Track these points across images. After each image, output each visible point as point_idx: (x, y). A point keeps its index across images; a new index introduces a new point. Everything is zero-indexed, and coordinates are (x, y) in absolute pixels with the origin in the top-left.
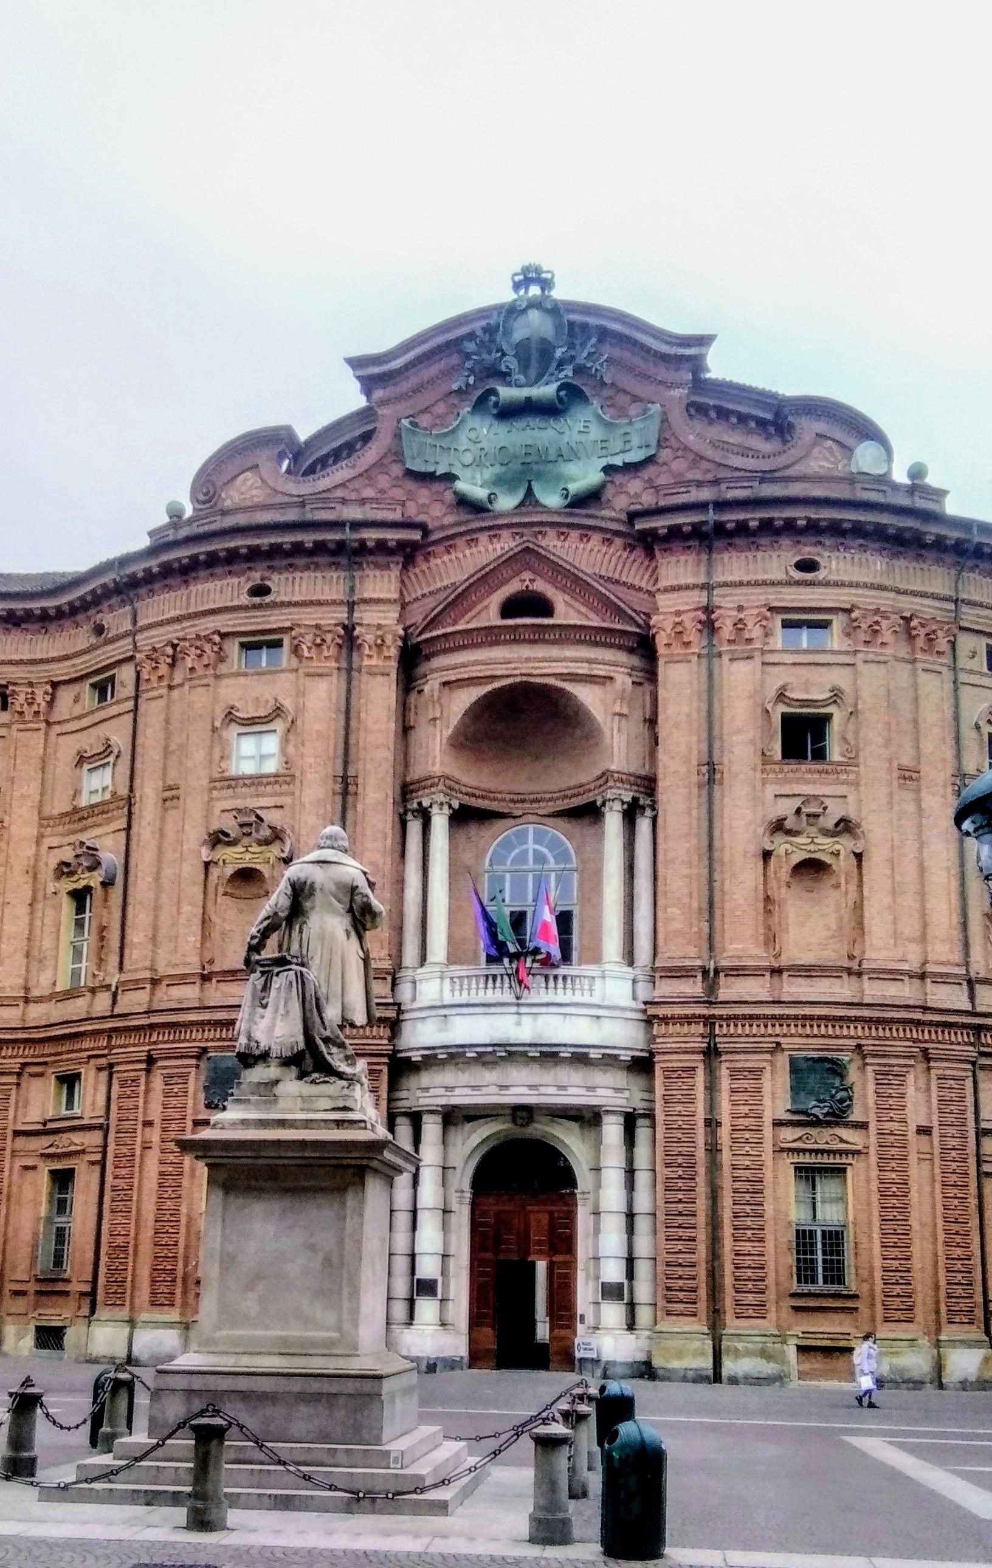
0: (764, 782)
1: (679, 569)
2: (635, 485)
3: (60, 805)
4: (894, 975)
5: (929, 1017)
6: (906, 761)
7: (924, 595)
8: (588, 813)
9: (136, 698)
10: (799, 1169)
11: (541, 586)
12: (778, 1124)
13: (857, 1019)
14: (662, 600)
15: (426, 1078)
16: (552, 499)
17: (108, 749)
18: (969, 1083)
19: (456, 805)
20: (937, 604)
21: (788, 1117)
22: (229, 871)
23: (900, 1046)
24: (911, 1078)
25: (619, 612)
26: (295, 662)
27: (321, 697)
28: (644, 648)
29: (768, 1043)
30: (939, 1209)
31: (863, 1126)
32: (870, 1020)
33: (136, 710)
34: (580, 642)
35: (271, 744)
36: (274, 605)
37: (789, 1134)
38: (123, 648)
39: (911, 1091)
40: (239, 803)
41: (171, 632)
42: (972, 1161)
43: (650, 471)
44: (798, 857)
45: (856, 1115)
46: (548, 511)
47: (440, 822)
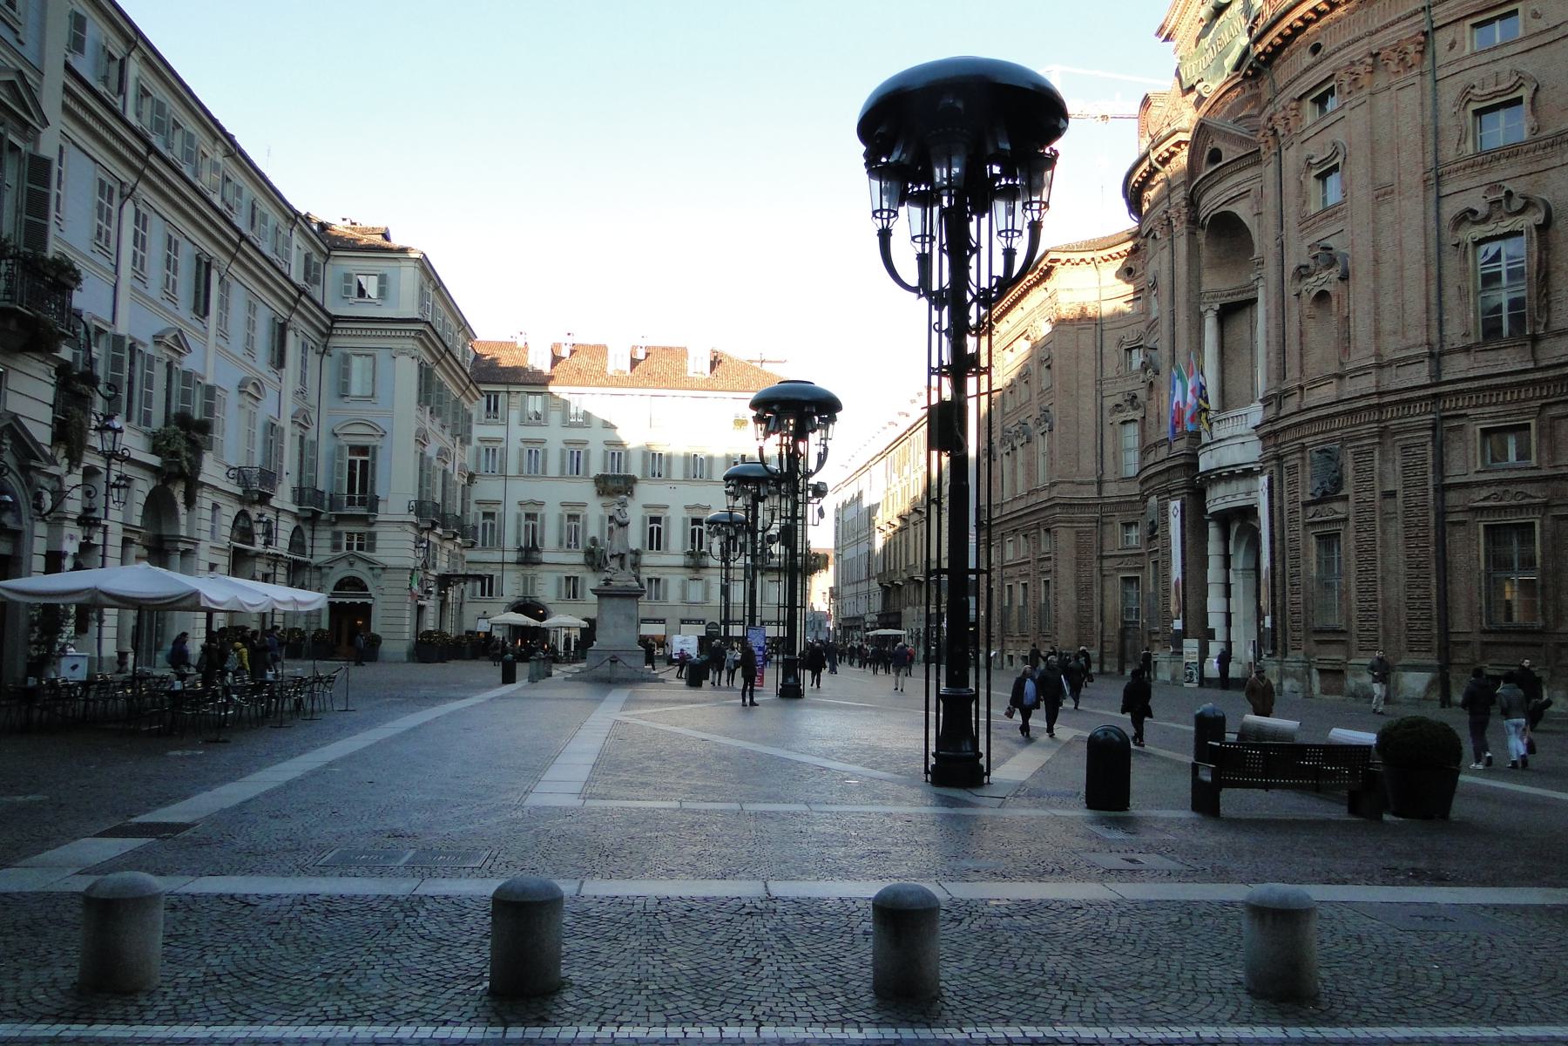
0: (1303, 238)
4: (1363, 371)
5: (1386, 399)
6: (1386, 178)
7: (1393, 24)
10: (1319, 537)
12: (1306, 505)
13: (1338, 414)
18: (1429, 447)
19: (1217, 307)
20: (1407, 23)
21: (1310, 498)
23: (1364, 430)
24: (1376, 454)
29: (1295, 445)
30: (1402, 558)
31: (1346, 498)
32: (1344, 413)
34: (1231, 173)
37: (1311, 510)
39: (1377, 463)
42: (1432, 514)
44: (1314, 293)
45: (1342, 493)
47: (1210, 323)
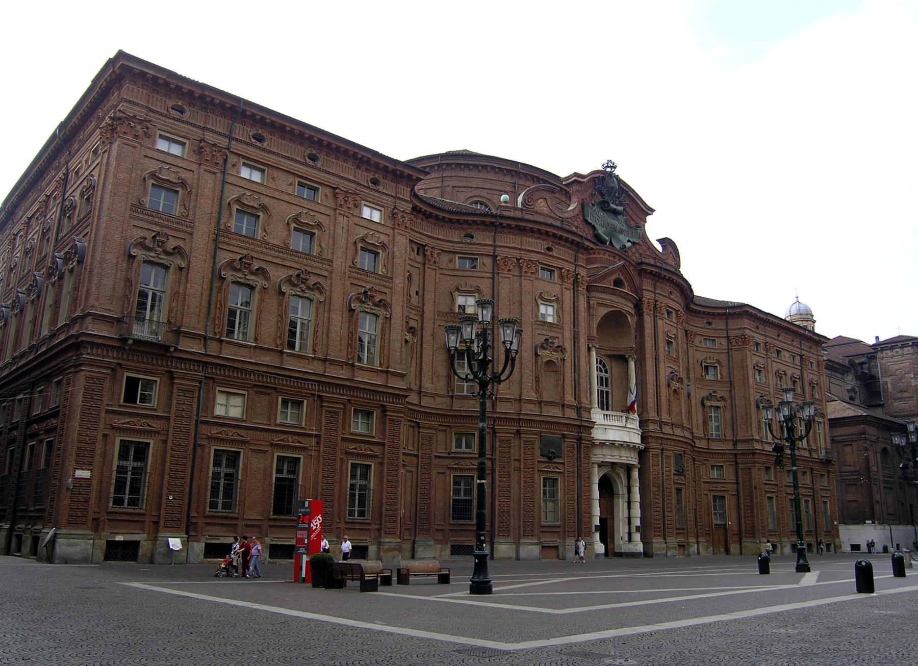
1: (647, 284)
2: (634, 250)
3: (444, 308)
8: (623, 359)
9: (493, 273)
11: (622, 278)
14: (645, 293)
15: (598, 451)
16: (618, 246)
17: (478, 290)
22: (544, 360)
25: (636, 294)
26: (560, 282)
27: (568, 296)
28: (638, 307)
33: (493, 278)
35: (550, 311)
36: (552, 256)
38: (490, 250)
40: (544, 332)
41: (516, 253)
43: (638, 247)
46: (616, 249)
